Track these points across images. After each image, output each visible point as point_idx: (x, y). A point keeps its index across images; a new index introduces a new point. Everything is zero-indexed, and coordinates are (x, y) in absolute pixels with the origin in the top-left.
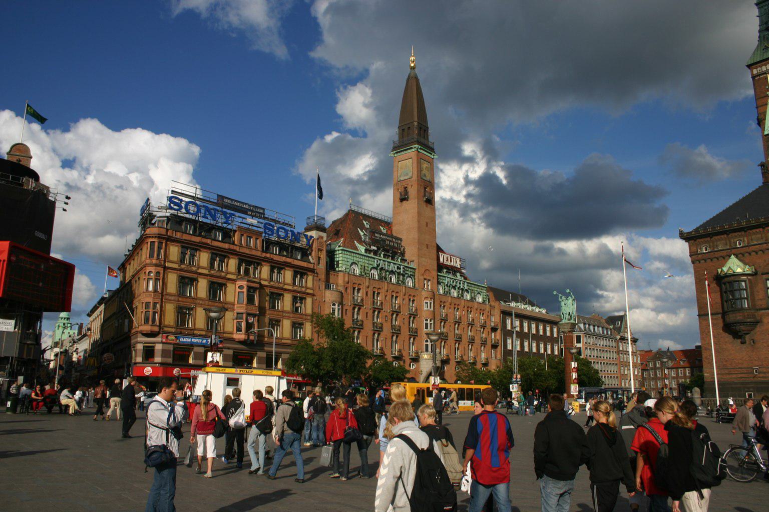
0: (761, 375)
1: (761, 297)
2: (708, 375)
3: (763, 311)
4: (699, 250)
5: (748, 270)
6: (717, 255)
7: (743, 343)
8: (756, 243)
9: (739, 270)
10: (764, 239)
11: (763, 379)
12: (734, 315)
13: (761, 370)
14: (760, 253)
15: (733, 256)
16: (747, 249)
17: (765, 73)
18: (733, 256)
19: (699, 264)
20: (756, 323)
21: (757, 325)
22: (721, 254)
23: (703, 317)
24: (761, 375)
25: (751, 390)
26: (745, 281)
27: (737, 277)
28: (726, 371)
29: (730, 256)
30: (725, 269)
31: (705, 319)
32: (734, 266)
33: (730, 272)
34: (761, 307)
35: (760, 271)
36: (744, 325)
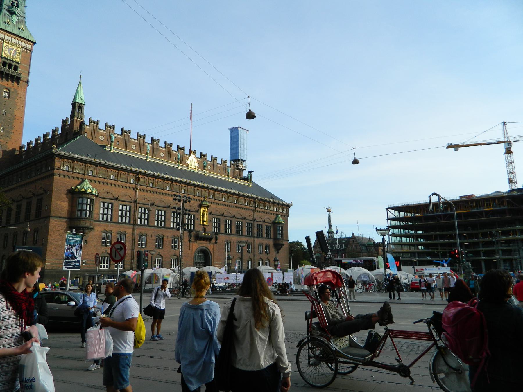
0: (87, 266)
2: (49, 264)
3: (96, 222)
4: (62, 167)
6: (75, 175)
8: (101, 176)
10: (106, 176)
11: (87, 268)
12: (85, 222)
13: (87, 262)
14: (101, 183)
16: (94, 178)
18: (87, 180)
19: (59, 177)
21: (91, 230)
22: (78, 175)
23: (54, 218)
24: (87, 266)
25: (79, 276)
26: (93, 200)
27: (92, 195)
31: (55, 220)
34: (96, 219)
35: (100, 195)
36: (89, 230)
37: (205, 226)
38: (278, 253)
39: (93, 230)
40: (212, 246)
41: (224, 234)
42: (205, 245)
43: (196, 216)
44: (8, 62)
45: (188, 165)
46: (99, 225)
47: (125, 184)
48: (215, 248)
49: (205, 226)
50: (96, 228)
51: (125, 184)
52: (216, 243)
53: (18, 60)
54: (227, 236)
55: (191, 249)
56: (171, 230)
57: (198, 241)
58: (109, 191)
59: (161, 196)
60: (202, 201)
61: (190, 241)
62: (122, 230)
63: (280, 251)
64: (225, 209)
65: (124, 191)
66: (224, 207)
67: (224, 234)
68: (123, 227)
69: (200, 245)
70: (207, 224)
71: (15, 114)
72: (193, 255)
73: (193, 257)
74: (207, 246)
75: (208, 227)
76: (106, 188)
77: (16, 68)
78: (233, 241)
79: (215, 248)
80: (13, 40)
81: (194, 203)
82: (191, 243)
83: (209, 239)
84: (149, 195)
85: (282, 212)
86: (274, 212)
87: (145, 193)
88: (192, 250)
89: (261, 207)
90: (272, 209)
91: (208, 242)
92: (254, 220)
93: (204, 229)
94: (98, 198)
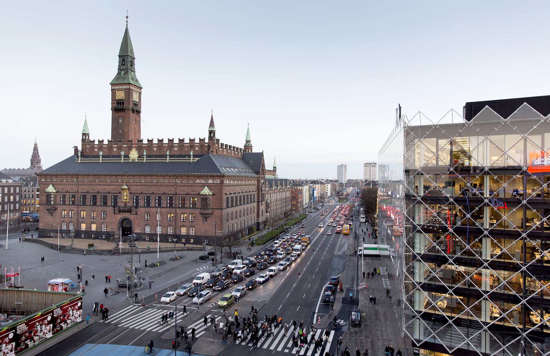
1: (58, 200)
5: (54, 191)
7: (52, 216)
9: (51, 191)
15: (51, 185)
17: (115, 90)
20: (56, 209)
28: (46, 225)
29: (49, 185)
30: (46, 189)
32: (51, 189)
33: (48, 191)
37: (126, 203)
38: (206, 221)
39: (57, 210)
40: (133, 216)
41: (143, 207)
42: (126, 216)
43: (119, 196)
44: (119, 101)
45: (129, 158)
46: (60, 207)
47: (72, 183)
48: (135, 218)
49: (126, 203)
50: (59, 209)
51: (72, 183)
52: (136, 214)
53: (124, 98)
54: (146, 208)
55: (116, 218)
56: (101, 207)
57: (121, 213)
58: (64, 188)
59: (94, 186)
60: (122, 185)
61: (115, 213)
62: (71, 209)
63: (208, 219)
64: (144, 188)
65: (71, 187)
66: (144, 187)
67: (143, 207)
68: (72, 207)
69: (123, 216)
70: (128, 201)
71: (125, 130)
72: (118, 221)
73: (117, 224)
74: (129, 216)
75: (129, 203)
76: (62, 187)
77: (123, 103)
78: (152, 212)
79: (135, 218)
80: (120, 87)
81: (117, 187)
82: (116, 215)
83: (130, 211)
84: (86, 187)
85: (213, 183)
86: (202, 184)
87: (83, 186)
88: (117, 219)
89: (184, 182)
90: (198, 181)
91: (130, 214)
92: (176, 194)
93: (125, 204)
94: (58, 193)
